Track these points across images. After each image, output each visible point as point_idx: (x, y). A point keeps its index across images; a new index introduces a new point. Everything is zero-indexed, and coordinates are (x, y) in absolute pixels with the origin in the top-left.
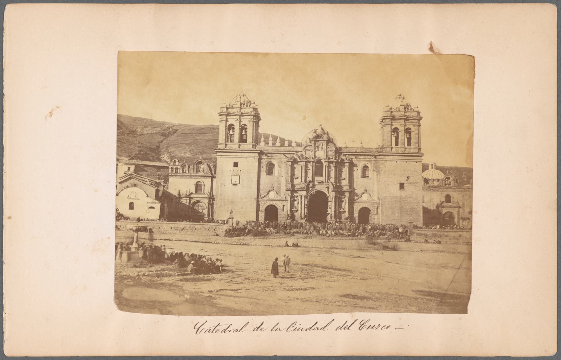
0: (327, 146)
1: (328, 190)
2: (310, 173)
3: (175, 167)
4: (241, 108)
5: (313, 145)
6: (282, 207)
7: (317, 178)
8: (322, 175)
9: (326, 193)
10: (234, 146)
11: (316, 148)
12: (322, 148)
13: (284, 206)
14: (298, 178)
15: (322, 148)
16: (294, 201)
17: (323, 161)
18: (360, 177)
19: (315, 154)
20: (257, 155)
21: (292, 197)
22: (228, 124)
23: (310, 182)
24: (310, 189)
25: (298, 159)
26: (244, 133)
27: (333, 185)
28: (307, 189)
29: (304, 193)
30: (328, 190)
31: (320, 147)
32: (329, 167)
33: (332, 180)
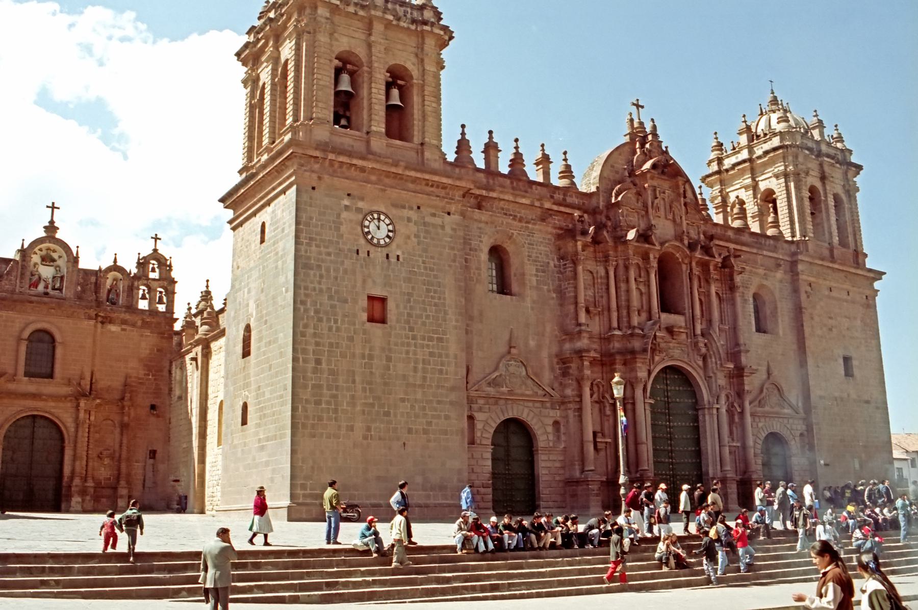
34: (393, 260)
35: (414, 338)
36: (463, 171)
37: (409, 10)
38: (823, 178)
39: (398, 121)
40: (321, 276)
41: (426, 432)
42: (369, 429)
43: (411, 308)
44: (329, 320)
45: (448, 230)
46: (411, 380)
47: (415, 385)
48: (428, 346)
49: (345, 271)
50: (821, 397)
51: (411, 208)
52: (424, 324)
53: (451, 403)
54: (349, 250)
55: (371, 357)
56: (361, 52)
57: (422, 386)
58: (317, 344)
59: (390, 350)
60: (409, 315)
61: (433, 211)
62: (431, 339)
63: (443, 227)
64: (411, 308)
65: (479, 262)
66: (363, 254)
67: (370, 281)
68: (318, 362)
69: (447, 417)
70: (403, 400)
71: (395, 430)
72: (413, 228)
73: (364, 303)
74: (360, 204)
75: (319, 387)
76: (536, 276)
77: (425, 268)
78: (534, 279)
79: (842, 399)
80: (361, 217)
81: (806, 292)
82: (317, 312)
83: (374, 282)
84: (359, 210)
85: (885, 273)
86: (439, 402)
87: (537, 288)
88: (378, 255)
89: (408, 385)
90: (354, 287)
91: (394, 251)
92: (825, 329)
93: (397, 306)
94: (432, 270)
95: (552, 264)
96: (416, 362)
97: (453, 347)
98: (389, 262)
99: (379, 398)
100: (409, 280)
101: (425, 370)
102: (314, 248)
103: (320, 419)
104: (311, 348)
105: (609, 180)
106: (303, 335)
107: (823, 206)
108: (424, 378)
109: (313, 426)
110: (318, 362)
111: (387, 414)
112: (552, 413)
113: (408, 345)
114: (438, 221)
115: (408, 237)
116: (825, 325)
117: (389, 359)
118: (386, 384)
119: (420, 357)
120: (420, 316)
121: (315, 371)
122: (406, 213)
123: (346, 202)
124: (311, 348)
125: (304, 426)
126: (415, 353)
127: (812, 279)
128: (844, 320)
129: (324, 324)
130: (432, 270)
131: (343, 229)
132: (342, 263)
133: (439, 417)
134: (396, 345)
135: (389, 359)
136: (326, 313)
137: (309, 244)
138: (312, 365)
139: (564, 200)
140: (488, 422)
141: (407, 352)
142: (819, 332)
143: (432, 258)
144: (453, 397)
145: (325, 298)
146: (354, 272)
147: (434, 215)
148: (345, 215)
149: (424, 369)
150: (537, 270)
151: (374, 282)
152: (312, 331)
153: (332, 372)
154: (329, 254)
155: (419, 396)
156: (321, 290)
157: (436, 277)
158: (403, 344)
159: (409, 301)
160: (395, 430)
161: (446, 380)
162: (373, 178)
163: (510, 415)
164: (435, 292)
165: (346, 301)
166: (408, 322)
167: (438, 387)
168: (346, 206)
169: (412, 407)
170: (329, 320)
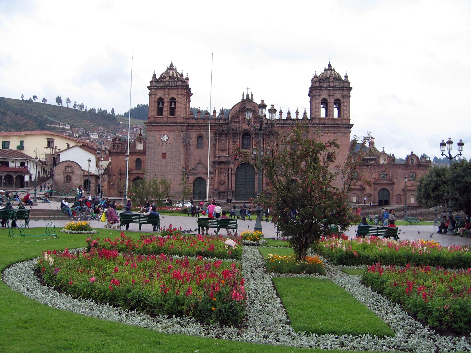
20: (185, 128)
34: (168, 144)
38: (329, 96)
39: (172, 111)
45: (182, 135)
56: (163, 97)
66: (161, 144)
68: (151, 168)
73: (161, 154)
84: (160, 134)
85: (353, 125)
88: (165, 144)
97: (182, 162)
101: (175, 168)
107: (328, 104)
110: (151, 168)
114: (180, 134)
122: (172, 133)
127: (313, 131)
135: (166, 166)
140: (192, 179)
148: (157, 136)
153: (154, 169)
163: (196, 177)
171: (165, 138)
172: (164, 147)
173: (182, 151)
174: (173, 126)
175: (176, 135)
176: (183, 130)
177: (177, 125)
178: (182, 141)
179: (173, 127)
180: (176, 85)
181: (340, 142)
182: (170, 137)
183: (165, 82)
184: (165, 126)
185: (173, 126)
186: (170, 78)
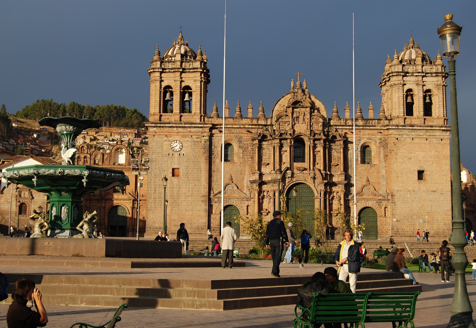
0: (311, 117)
1: (314, 182)
2: (286, 158)
3: (82, 156)
4: (182, 62)
5: (290, 115)
6: (245, 208)
7: (296, 165)
8: (304, 161)
9: (312, 186)
10: (174, 117)
11: (295, 120)
12: (304, 120)
13: (248, 206)
14: (268, 164)
15: (304, 120)
16: (263, 198)
17: (306, 139)
18: (359, 162)
19: (293, 127)
20: (207, 130)
21: (260, 192)
22: (164, 84)
23: (287, 169)
24: (287, 180)
25: (268, 136)
26: (187, 98)
27: (322, 174)
28: (283, 179)
29: (276, 187)
30: (314, 182)
31: (301, 117)
32: (315, 147)
33: (320, 166)
34: (182, 155)
35: (189, 180)
36: (213, 119)
37: (191, 63)
40: (156, 164)
41: (192, 211)
42: (172, 210)
43: (188, 171)
44: (159, 177)
45: (203, 142)
46: (187, 194)
47: (188, 196)
48: (194, 183)
49: (165, 161)
50: (398, 191)
51: (189, 137)
52: (192, 175)
53: (202, 201)
54: (166, 154)
55: (173, 188)
57: (191, 196)
58: (155, 185)
59: (180, 185)
60: (187, 173)
61: (197, 136)
62: (195, 180)
63: (201, 142)
64: (188, 171)
65: (218, 151)
67: (173, 163)
68: (155, 190)
69: (200, 206)
70: (184, 201)
71: (181, 210)
72: (189, 144)
73: (171, 171)
74: (170, 139)
75: (156, 198)
76: (243, 153)
77: (194, 157)
78: (241, 155)
79: (414, 191)
80: (170, 143)
81: (394, 143)
82: (155, 175)
83: (175, 164)
84: (169, 141)
86: (197, 201)
87: (242, 158)
88: (176, 155)
89: (186, 196)
90: (167, 166)
91: (182, 152)
92: (405, 159)
93: (183, 171)
94: (196, 157)
95: (250, 148)
96: (189, 188)
98: (180, 157)
99: (176, 200)
100: (187, 162)
102: (154, 155)
103: (156, 208)
104: (153, 186)
105: (278, 111)
106: (150, 182)
108: (192, 193)
109: (153, 210)
111: (178, 205)
112: (246, 202)
113: (187, 183)
114: (199, 140)
115: (188, 147)
116: (406, 157)
117: (179, 188)
118: (178, 196)
119: (191, 187)
120: (190, 173)
121: (154, 193)
122: (187, 139)
123: (165, 139)
124: (153, 186)
125: (151, 210)
126: (189, 185)
128: (421, 153)
129: (157, 179)
130: (196, 157)
131: (164, 147)
132: (164, 159)
133: (197, 206)
134: (182, 183)
135: (179, 188)
136: (158, 175)
137: (152, 154)
138: (152, 192)
139: (257, 122)
141: (186, 185)
142: (401, 161)
143: (196, 153)
144: (203, 199)
145: (158, 171)
146: (168, 161)
147: (197, 138)
148: (165, 143)
149: (192, 190)
150: (243, 151)
151: (175, 164)
152: (153, 181)
154: (159, 156)
155: (190, 199)
156: (156, 168)
157: (197, 159)
158: (184, 183)
159: (187, 168)
160: (181, 210)
161: (200, 193)
162: (175, 129)
164: (197, 164)
165: (165, 171)
166: (187, 175)
167: (197, 196)
168: (165, 140)
169: (188, 203)
170: (159, 177)
171: (177, 146)
172: (176, 160)
173: (204, 166)
174: (190, 127)
175: (194, 142)
176: (205, 134)
177: (195, 127)
178: (202, 150)
179: (189, 129)
180: (191, 67)
181: (436, 151)
182: (185, 145)
183: (174, 62)
184: (177, 127)
185: (190, 127)
186: (182, 56)
